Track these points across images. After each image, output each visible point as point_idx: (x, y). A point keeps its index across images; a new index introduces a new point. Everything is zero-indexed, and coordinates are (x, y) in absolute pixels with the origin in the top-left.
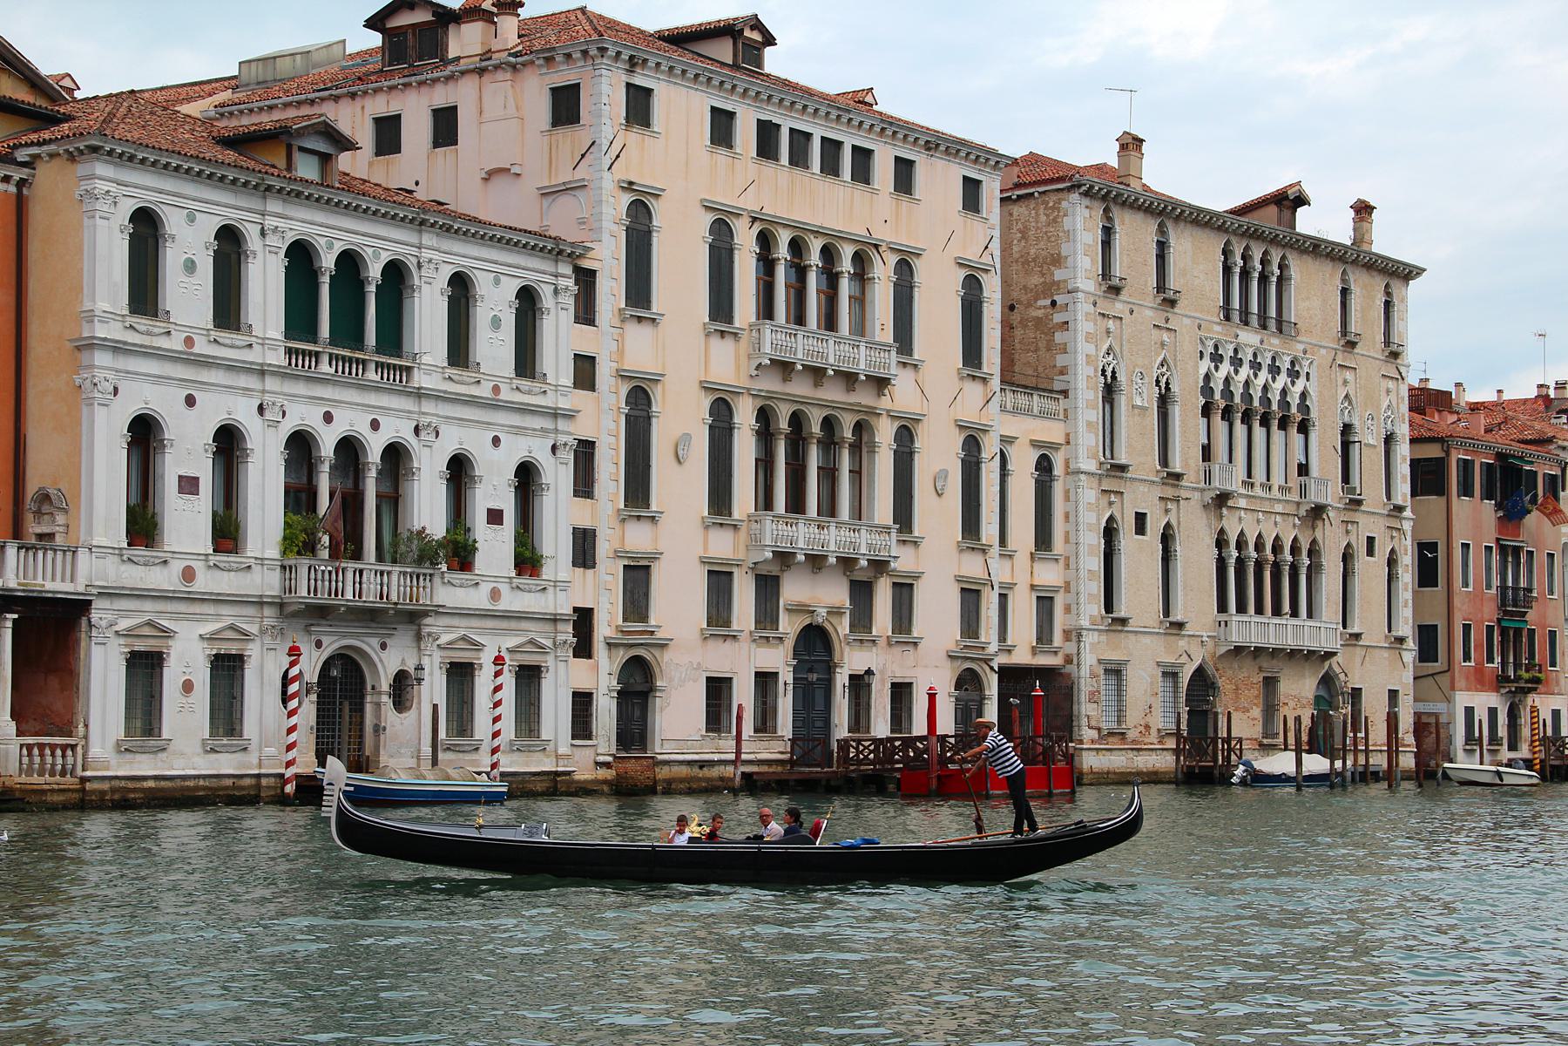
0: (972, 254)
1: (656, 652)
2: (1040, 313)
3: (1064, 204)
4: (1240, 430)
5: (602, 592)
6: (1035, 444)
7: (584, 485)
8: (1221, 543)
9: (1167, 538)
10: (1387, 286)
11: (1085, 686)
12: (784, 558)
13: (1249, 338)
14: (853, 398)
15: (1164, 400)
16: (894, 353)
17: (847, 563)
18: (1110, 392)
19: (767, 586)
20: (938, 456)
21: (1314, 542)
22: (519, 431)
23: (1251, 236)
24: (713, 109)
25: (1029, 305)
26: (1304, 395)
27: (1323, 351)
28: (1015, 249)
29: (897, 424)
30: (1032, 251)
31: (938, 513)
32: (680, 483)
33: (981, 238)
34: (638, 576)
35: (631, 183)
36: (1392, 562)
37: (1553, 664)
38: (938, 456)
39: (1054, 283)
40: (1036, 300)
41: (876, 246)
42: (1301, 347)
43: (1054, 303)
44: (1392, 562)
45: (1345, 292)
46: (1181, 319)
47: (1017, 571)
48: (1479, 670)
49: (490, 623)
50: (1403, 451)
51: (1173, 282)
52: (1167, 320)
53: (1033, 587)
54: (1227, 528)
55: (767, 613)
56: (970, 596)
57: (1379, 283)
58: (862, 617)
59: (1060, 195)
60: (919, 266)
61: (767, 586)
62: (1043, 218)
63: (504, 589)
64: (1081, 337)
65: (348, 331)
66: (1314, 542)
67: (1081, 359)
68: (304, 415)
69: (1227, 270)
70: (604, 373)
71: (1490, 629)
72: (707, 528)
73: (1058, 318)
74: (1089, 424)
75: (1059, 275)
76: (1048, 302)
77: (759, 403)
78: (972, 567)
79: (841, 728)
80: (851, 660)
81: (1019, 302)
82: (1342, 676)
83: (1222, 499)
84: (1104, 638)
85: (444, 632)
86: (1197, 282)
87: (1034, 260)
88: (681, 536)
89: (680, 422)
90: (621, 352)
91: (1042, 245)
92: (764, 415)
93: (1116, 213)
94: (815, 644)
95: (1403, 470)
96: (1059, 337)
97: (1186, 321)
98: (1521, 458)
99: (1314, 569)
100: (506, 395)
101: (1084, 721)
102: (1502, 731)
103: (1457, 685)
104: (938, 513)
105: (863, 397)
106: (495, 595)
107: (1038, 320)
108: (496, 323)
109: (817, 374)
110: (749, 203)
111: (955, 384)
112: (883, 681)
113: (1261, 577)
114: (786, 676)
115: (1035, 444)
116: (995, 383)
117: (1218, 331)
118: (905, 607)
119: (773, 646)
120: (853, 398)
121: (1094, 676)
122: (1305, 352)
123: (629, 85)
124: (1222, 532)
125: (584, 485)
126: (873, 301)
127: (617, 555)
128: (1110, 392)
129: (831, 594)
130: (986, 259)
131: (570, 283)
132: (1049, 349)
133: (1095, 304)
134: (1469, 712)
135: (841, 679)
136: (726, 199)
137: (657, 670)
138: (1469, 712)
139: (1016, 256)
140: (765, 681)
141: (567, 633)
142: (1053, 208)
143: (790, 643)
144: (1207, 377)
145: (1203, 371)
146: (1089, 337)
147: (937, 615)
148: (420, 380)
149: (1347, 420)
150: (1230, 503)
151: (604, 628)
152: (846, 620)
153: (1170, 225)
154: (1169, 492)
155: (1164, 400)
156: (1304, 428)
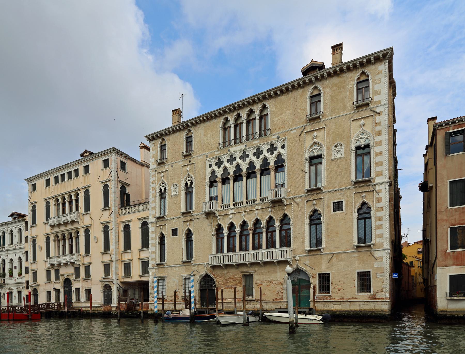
5: (30, 277)
6: (139, 219)
8: (219, 229)
9: (189, 234)
12: (59, 265)
17: (73, 263)
18: (162, 195)
19: (57, 272)
31: (97, 247)
32: (41, 255)
34: (35, 273)
53: (139, 259)
55: (57, 278)
61: (57, 272)
72: (32, 263)
78: (107, 258)
104: (97, 247)
106: (15, 280)
109: (66, 224)
111: (101, 213)
115: (139, 219)
127: (31, 270)
128: (162, 195)
146: (153, 182)
151: (30, 284)
154: (189, 218)
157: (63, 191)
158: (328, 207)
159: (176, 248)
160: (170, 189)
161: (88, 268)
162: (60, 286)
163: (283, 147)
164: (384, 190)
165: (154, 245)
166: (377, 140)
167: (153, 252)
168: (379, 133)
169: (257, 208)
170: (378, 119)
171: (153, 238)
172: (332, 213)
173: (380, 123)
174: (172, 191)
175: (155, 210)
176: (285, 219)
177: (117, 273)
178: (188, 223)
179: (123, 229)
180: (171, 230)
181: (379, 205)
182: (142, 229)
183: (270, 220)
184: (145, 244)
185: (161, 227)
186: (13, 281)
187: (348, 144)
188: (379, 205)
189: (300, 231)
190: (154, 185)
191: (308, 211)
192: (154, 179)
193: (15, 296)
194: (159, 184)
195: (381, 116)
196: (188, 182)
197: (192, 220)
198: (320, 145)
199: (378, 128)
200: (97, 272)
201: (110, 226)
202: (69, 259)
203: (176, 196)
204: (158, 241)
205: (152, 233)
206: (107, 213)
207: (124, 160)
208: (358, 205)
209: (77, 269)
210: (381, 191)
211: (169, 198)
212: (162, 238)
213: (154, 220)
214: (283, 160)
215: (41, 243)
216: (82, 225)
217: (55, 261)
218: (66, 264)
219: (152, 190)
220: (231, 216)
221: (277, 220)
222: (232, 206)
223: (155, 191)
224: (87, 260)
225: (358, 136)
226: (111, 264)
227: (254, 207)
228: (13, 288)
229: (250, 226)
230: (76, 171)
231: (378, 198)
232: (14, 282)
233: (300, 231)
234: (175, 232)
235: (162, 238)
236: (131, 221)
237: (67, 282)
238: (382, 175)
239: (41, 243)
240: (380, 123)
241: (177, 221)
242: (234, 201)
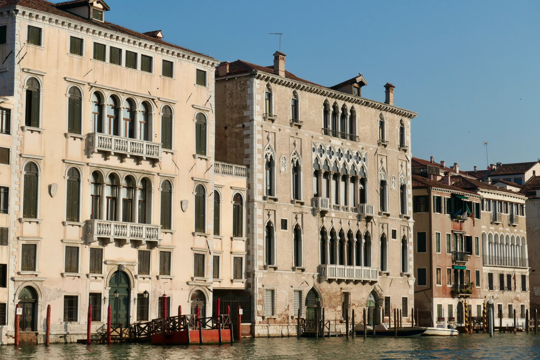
0: (200, 104)
2: (237, 130)
3: (248, 82)
4: (342, 184)
8: (323, 232)
10: (401, 121)
11: (258, 297)
14: (140, 167)
15: (296, 169)
16: (160, 147)
18: (270, 165)
20: (184, 194)
21: (367, 232)
23: (336, 98)
24: (71, 37)
25: (233, 127)
26: (363, 167)
27: (371, 149)
28: (227, 102)
30: (235, 103)
33: (206, 97)
35: (29, 70)
36: (404, 242)
37: (478, 284)
38: (184, 194)
39: (245, 117)
40: (236, 124)
41: (153, 99)
42: (361, 147)
43: (244, 126)
44: (404, 242)
45: (382, 124)
46: (305, 133)
47: (227, 246)
48: (444, 287)
50: (409, 192)
51: (300, 118)
52: (297, 134)
54: (326, 226)
56: (199, 260)
57: (398, 118)
59: (246, 78)
60: (175, 109)
62: (239, 88)
64: (255, 141)
66: (367, 232)
67: (255, 151)
69: (326, 112)
71: (449, 270)
73: (245, 132)
74: (259, 180)
75: (246, 113)
76: (241, 125)
77: (94, 169)
79: (134, 319)
80: (139, 286)
81: (229, 125)
82: (380, 291)
83: (323, 213)
84: (265, 276)
86: (311, 117)
87: (235, 107)
88: (52, 230)
89: (53, 177)
90: (22, 145)
91: (239, 100)
92: (97, 175)
93: (272, 85)
95: (409, 201)
96: (246, 141)
98: (463, 196)
99: (368, 244)
101: (256, 312)
102: (455, 315)
103: (434, 295)
107: (237, 134)
110: (90, 79)
112: (155, 296)
113: (343, 248)
114: (106, 294)
116: (212, 161)
117: (321, 139)
118: (167, 264)
119: (100, 281)
120: (140, 167)
121: (260, 293)
122: (363, 149)
123: (29, 27)
124: (323, 228)
126: (151, 124)
129: (128, 256)
130: (208, 106)
132: (241, 146)
133: (262, 126)
134: (440, 306)
135: (134, 295)
137: (39, 293)
138: (440, 306)
139: (228, 105)
140: (95, 298)
142: (243, 84)
143: (107, 280)
144: (317, 159)
145: (314, 157)
147: (183, 267)
149: (383, 179)
150: (326, 215)
153: (298, 91)
155: (296, 169)
156: (363, 181)
162: (101, 286)
218: (120, 243)
236: (221, 187)
237: (121, 278)
241: (286, 209)
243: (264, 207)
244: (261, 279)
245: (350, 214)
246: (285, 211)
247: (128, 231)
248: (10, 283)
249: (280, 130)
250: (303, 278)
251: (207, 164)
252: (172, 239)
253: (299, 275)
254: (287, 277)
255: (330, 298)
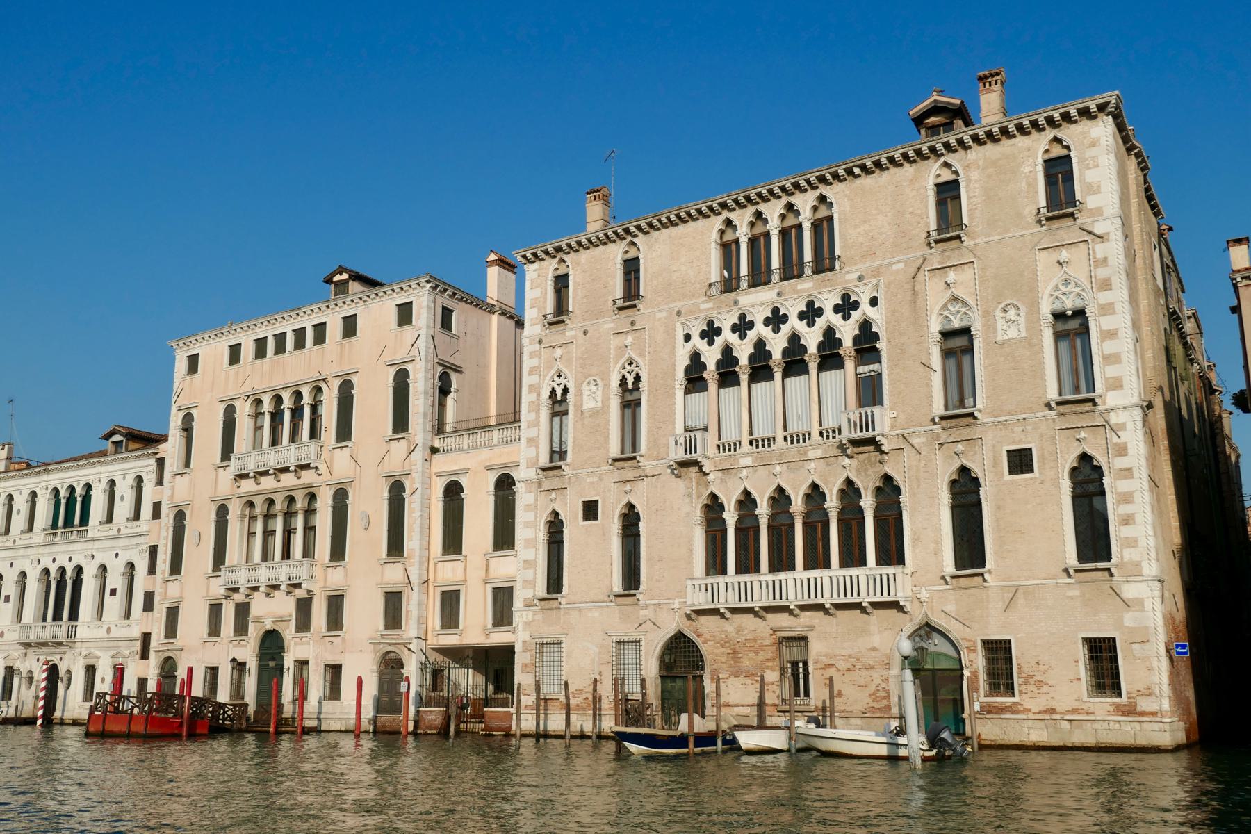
1: (177, 653)
5: (156, 624)
7: (152, 570)
13: (757, 302)
18: (558, 404)
19: (242, 610)
22: (126, 548)
29: (332, 491)
34: (173, 613)
41: (324, 380)
49: (105, 644)
52: (633, 323)
58: (304, 623)
63: (113, 628)
65: (68, 522)
68: (46, 562)
70: (164, 510)
78: (393, 575)
85: (81, 649)
90: (172, 496)
94: (272, 644)
97: (659, 315)
100: (124, 531)
105: (307, 477)
106: (109, 630)
108: (122, 498)
110: (247, 389)
111: (385, 447)
112: (317, 664)
114: (252, 665)
122: (860, 278)
125: (152, 570)
131: (155, 467)
133: (540, 342)
135: (289, 662)
136: (231, 394)
140: (239, 667)
141: (138, 645)
148: (90, 534)
151: (154, 644)
152: (293, 624)
154: (630, 474)
157: (277, 382)
158: (996, 464)
159: (594, 553)
160: (579, 394)
161: (336, 604)
163: (874, 302)
164: (1130, 426)
165: (530, 543)
166: (1102, 301)
167: (529, 564)
168: (1106, 285)
169: (811, 454)
170: (1100, 249)
171: (527, 525)
172: (1007, 477)
173: (1105, 260)
174: (585, 397)
175: (537, 447)
176: (888, 490)
177: (421, 615)
178: (628, 487)
179: (441, 494)
180: (580, 504)
181: (1120, 462)
182: (496, 496)
183: (850, 491)
184: (504, 537)
185: (553, 495)
186: (101, 633)
187: (1034, 306)
188: (1120, 462)
189: (929, 525)
190: (535, 379)
191: (945, 471)
192: (535, 362)
193: (103, 680)
194: (548, 378)
195: (1106, 244)
196: (627, 376)
197: (639, 478)
198: (965, 304)
199: (1101, 273)
200: (365, 614)
201: (407, 484)
202: (284, 572)
203: (595, 413)
204: (542, 534)
205: (526, 510)
206: (400, 447)
207: (450, 304)
208: (1070, 460)
209: (304, 607)
210: (1123, 426)
211: (575, 416)
212: (555, 527)
213: (532, 473)
214: (876, 337)
215: (201, 528)
216: (326, 477)
217: (243, 578)
219: (531, 392)
220: (745, 472)
221: (866, 489)
222: (746, 446)
223: (539, 395)
224: (336, 578)
225: (1057, 288)
226: (406, 591)
227: (805, 453)
228: (98, 653)
229: (797, 505)
230: (320, 329)
231: (1116, 444)
232: (106, 635)
233: (929, 525)
234: (590, 511)
235: (555, 527)
236: (464, 472)
238: (1121, 387)
239: (201, 528)
240: (1105, 260)
241: (596, 479)
242: (751, 434)
243: (540, 487)
244: (527, 624)
245: (814, 447)
246: (592, 483)
247: (284, 572)
248: (152, 655)
249: (585, 333)
250: (642, 613)
251: (409, 446)
252: (346, 575)
253: (631, 608)
254: (596, 614)
255: (735, 652)
